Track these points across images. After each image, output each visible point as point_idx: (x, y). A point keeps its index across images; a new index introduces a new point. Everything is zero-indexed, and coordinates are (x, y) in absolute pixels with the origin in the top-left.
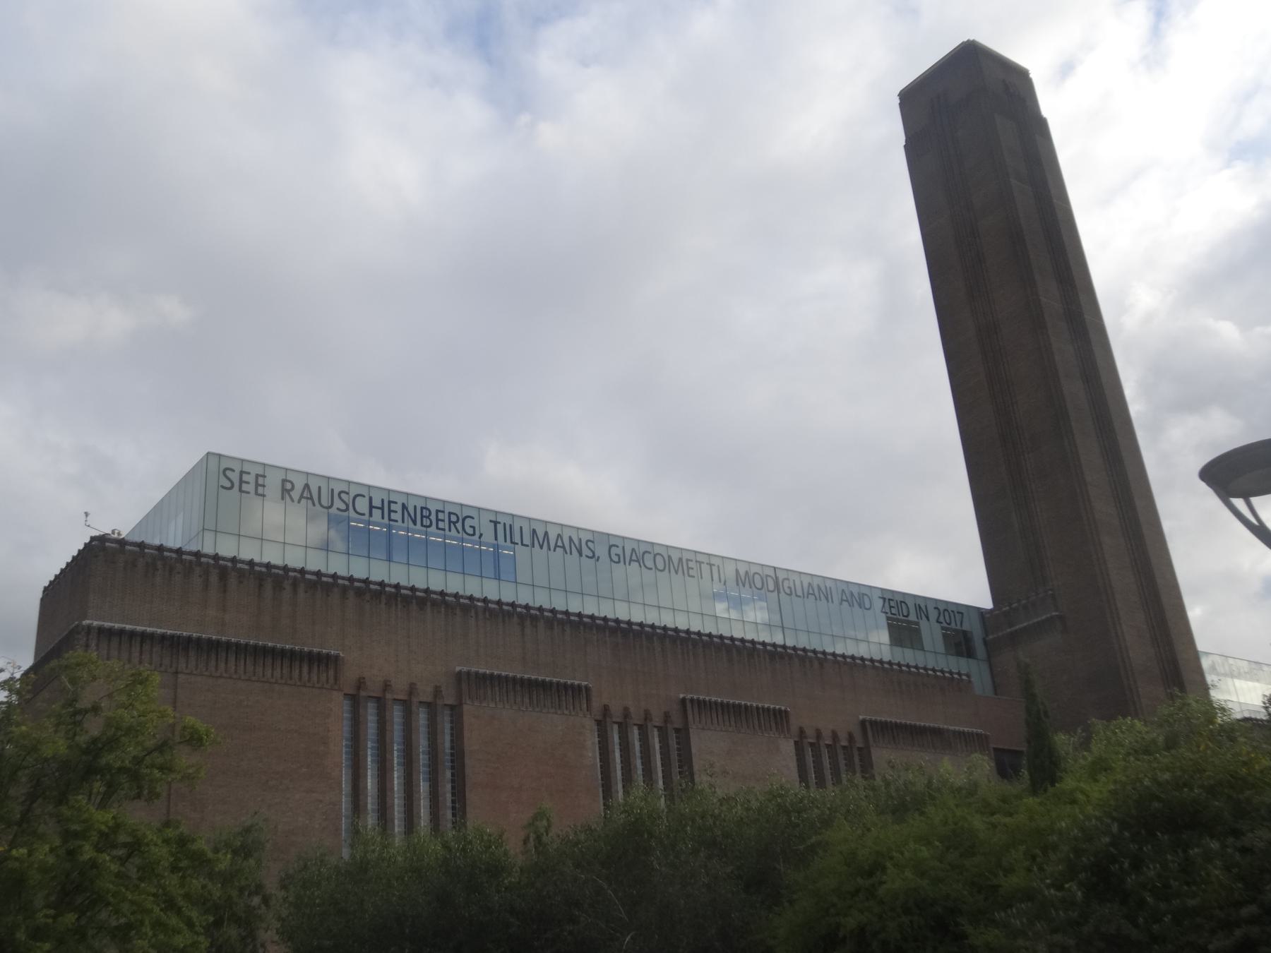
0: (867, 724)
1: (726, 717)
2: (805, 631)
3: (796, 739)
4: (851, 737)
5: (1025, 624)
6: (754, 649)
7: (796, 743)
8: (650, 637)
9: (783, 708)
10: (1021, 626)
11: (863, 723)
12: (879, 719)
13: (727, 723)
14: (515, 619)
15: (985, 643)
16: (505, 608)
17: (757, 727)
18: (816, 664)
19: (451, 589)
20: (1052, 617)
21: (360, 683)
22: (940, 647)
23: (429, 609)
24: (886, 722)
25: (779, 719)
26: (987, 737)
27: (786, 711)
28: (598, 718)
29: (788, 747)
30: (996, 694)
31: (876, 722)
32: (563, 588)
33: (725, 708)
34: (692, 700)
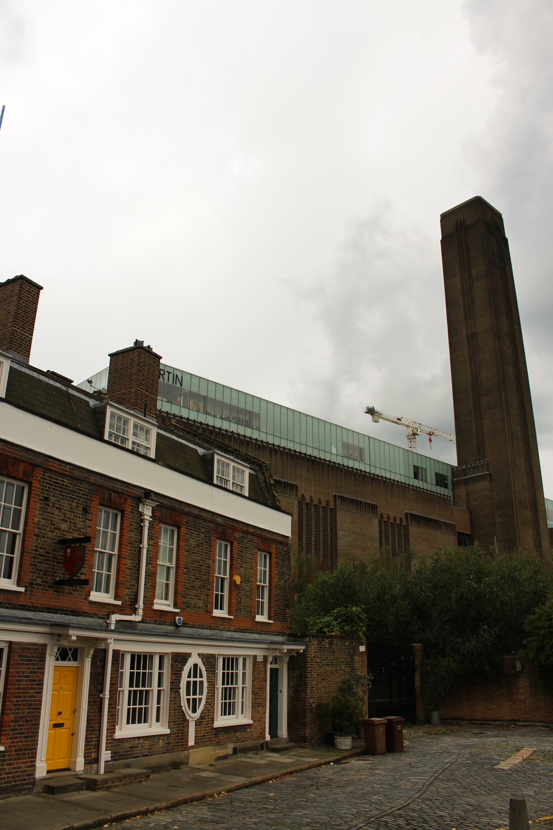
0: (409, 515)
1: (352, 505)
3: (379, 519)
4: (401, 520)
6: (365, 475)
7: (379, 520)
8: (323, 465)
10: (471, 476)
11: (407, 514)
12: (413, 513)
13: (352, 508)
14: (268, 450)
15: (452, 481)
16: (264, 444)
17: (364, 511)
18: (390, 485)
19: (254, 437)
20: (486, 474)
23: (233, 441)
25: (374, 508)
26: (455, 526)
27: (376, 506)
28: (300, 500)
29: (376, 522)
31: (412, 514)
33: (352, 501)
34: (339, 496)
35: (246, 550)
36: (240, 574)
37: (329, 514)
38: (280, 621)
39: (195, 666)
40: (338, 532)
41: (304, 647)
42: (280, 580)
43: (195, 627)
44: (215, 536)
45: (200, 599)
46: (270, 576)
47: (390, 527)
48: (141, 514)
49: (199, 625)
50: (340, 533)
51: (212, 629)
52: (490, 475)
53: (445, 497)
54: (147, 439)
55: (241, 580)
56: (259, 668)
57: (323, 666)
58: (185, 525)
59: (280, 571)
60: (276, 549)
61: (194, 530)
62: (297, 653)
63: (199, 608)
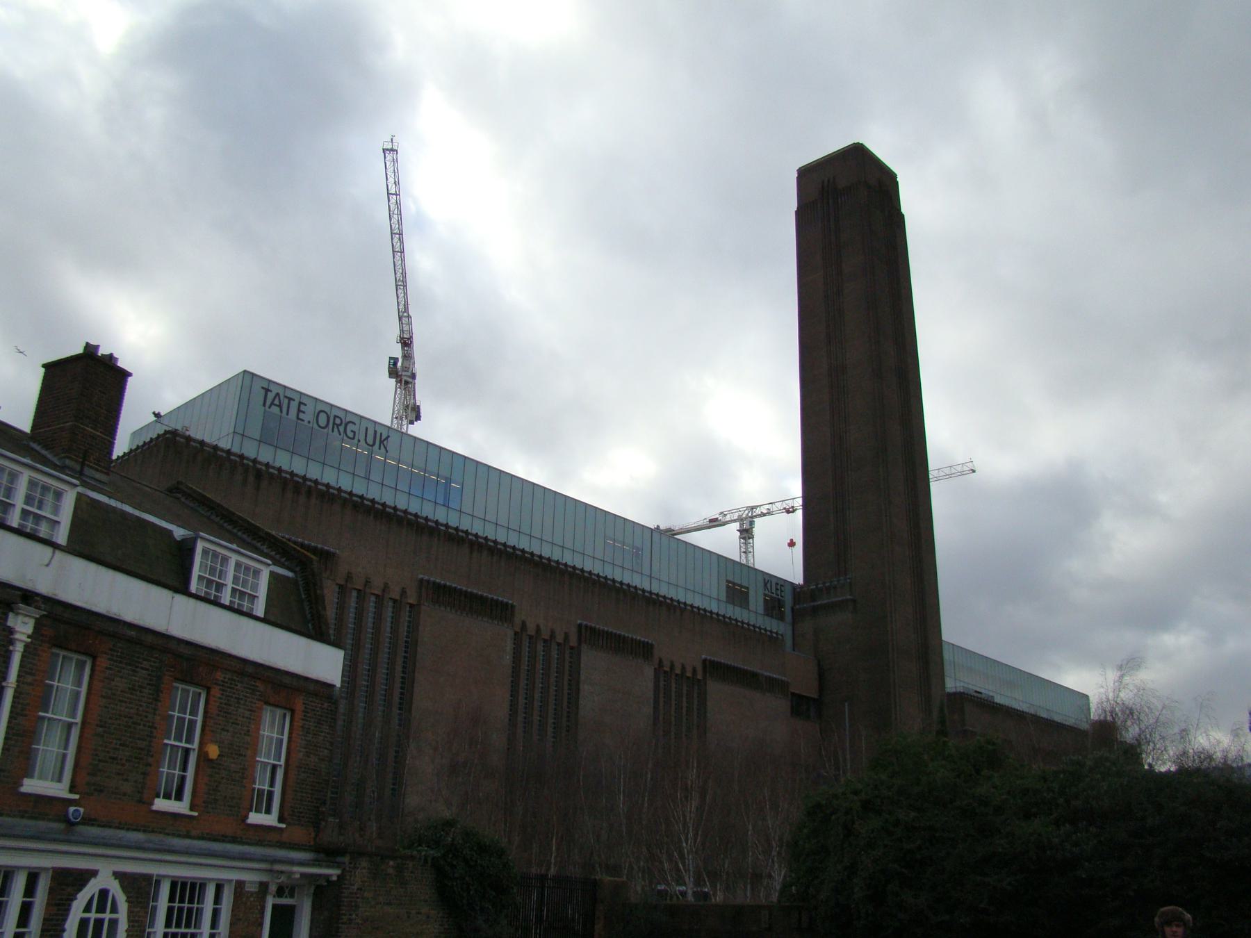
2: (666, 582)
4: (694, 671)
5: (825, 602)
7: (655, 669)
9: (650, 641)
11: (704, 661)
12: (716, 659)
15: (793, 609)
20: (847, 600)
21: (349, 577)
22: (761, 610)
24: (721, 663)
25: (645, 650)
29: (649, 672)
30: (794, 650)
32: (506, 525)
34: (586, 626)
35: (239, 703)
36: (220, 743)
37: (567, 656)
38: (302, 825)
39: (104, 893)
40: (581, 687)
41: (338, 872)
42: (309, 757)
43: (110, 827)
44: (171, 676)
45: (127, 780)
46: (288, 748)
47: (673, 681)
48: (11, 631)
49: (120, 823)
50: (585, 688)
51: (150, 832)
52: (854, 601)
53: (774, 635)
54: (56, 510)
55: (221, 751)
56: (249, 903)
57: (380, 906)
58: (106, 653)
59: (310, 741)
60: (304, 704)
61: (126, 664)
62: (328, 881)
63: (125, 794)
